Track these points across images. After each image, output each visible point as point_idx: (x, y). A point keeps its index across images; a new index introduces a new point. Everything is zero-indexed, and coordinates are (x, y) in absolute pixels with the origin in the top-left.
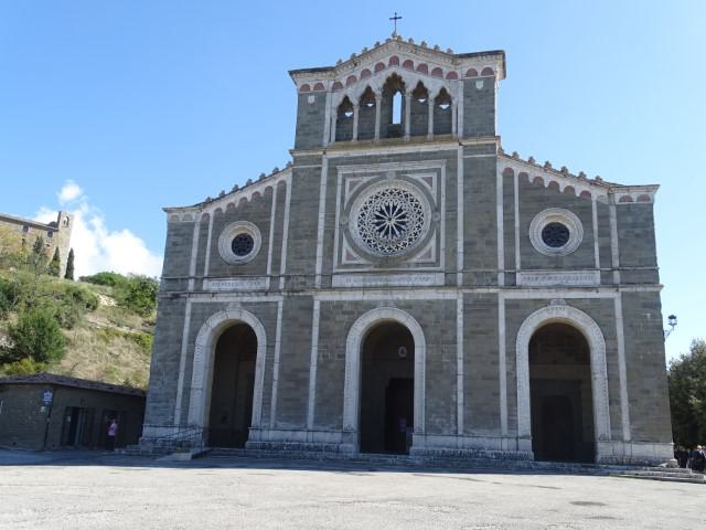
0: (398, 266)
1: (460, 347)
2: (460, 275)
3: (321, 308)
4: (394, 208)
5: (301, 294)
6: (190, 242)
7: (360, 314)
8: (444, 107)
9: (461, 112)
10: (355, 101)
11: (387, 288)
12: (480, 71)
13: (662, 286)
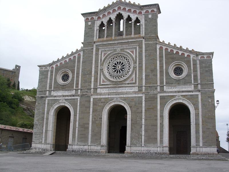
1: (143, 114)
2: (144, 88)
3: (93, 101)
4: (120, 62)
7: (107, 103)
8: (138, 24)
9: (144, 26)
10: (106, 24)
12: (150, 11)
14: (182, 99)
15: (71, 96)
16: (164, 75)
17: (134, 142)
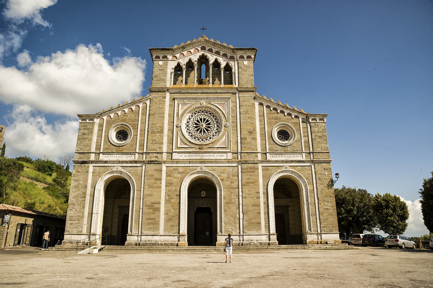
6: (91, 132)
7: (187, 173)
17: (228, 228)
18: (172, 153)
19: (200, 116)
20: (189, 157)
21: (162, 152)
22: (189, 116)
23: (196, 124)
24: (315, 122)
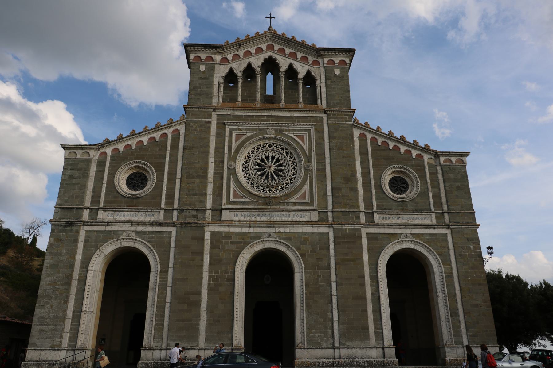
0: (278, 204)
2: (330, 214)
3: (212, 239)
4: (273, 158)
5: (194, 225)
6: (86, 176)
7: (247, 244)
9: (324, 90)
11: (271, 224)
13: (479, 225)
14: (415, 241)
15: (153, 226)
16: (373, 191)
18: (221, 210)
19: (266, 152)
20: (248, 216)
21: (204, 208)
22: (249, 153)
23: (259, 165)
24: (450, 165)
